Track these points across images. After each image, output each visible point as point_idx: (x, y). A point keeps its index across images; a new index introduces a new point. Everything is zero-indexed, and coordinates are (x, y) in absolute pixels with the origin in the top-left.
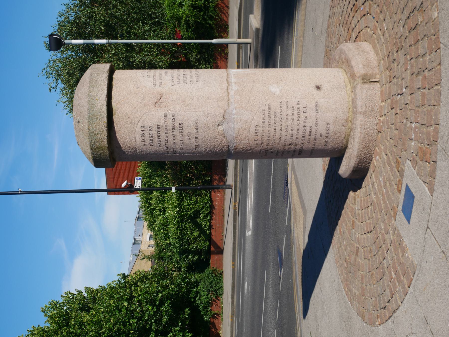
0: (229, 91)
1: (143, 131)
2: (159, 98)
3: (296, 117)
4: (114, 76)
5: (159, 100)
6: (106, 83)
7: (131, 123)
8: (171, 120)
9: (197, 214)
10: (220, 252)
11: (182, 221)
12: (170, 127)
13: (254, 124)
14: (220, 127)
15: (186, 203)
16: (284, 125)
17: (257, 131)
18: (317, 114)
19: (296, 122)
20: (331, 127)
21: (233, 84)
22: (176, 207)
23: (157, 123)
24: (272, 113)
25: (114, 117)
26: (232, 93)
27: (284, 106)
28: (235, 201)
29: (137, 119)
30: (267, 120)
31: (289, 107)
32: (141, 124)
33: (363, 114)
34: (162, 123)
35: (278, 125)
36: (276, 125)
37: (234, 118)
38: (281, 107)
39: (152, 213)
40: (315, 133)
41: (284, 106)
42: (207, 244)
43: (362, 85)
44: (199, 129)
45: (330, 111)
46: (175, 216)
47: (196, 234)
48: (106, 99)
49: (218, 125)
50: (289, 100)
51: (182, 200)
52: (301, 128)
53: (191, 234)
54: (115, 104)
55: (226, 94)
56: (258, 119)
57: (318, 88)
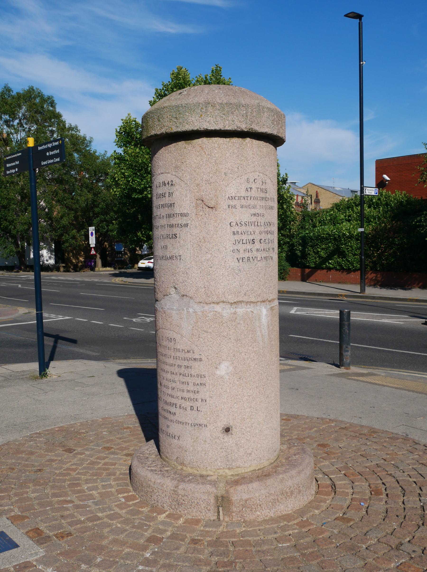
0: (221, 305)
1: (168, 184)
2: (209, 205)
3: (185, 395)
4: (248, 139)
5: (207, 206)
6: (228, 128)
7: (177, 167)
8: (180, 222)
9: (342, 254)
10: (304, 278)
11: (335, 239)
12: (173, 221)
13: (177, 337)
14: (174, 289)
15: (354, 244)
16: (177, 378)
17: (170, 340)
18: (190, 424)
19: (179, 394)
20: (176, 441)
21: (233, 311)
22: (350, 233)
23: (176, 203)
24: (191, 363)
25: (183, 142)
26: (218, 308)
27: (198, 381)
28: (346, 296)
29: (180, 174)
30: (181, 355)
31: (198, 387)
32: (176, 181)
33: (174, 491)
34: (177, 210)
35: (176, 370)
36: (176, 366)
37: (183, 310)
38: (198, 376)
39: (348, 208)
40: (170, 418)
41: (198, 381)
42: (313, 265)
43: (213, 495)
44: (170, 261)
45: (194, 442)
46: (340, 232)
47: (322, 254)
48: (202, 129)
49: (175, 288)
50: (207, 387)
51: (357, 240)
52: (173, 401)
53: (323, 249)
54: (200, 143)
55: (215, 299)
56: (183, 344)
57: (227, 430)
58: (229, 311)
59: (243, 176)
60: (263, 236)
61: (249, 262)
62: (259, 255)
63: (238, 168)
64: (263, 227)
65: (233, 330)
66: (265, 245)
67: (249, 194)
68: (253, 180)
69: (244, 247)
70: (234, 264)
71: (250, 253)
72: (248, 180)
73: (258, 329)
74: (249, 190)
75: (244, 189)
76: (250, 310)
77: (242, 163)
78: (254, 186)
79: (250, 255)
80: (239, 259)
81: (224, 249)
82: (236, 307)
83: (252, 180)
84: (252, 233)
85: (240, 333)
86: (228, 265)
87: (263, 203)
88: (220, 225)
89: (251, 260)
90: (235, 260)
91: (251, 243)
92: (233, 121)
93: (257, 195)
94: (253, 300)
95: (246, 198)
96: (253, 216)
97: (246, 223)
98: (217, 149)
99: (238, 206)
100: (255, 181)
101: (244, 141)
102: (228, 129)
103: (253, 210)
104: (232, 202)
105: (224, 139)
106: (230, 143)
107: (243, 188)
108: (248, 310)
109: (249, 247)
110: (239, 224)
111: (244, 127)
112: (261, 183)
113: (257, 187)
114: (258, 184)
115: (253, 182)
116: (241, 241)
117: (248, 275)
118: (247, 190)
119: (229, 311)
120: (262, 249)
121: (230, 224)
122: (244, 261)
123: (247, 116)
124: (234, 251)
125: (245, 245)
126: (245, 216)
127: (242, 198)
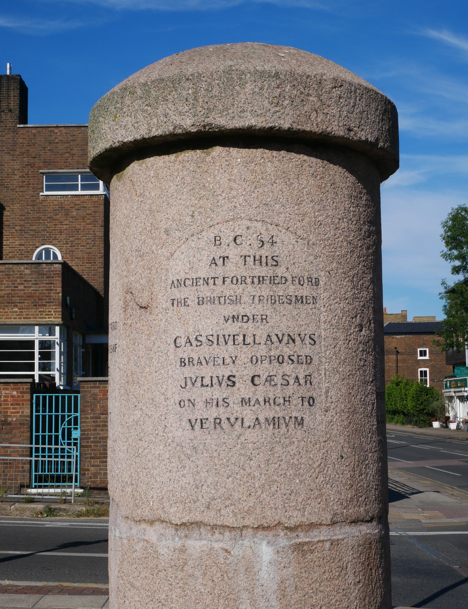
0: (157, 526)
4: (217, 150)
21: (178, 543)
26: (152, 533)
55: (147, 514)
58: (170, 544)
59: (204, 233)
60: (263, 370)
62: (248, 415)
63: (193, 216)
64: (263, 347)
65: (179, 590)
66: (272, 389)
67: (220, 271)
68: (232, 239)
69: (207, 393)
70: (181, 433)
71: (222, 409)
72: (217, 241)
73: (245, 595)
74: (220, 262)
75: (206, 260)
76: (221, 545)
77: (201, 202)
78: (233, 252)
79: (222, 412)
80: (193, 421)
81: (162, 398)
82: (186, 536)
83: (227, 238)
84: (228, 360)
85: (193, 598)
86: (170, 435)
87: (265, 290)
88: (156, 346)
89: (225, 425)
90: (183, 424)
91: (224, 384)
92: (166, 116)
93: (242, 272)
94: (230, 521)
96: (230, 321)
97: (211, 338)
98: (153, 180)
99: (192, 301)
100: (238, 241)
101: (208, 154)
102: (156, 134)
103: (230, 307)
104: (180, 291)
105: (166, 158)
106: (177, 163)
107: (205, 258)
108: (217, 546)
109: (217, 393)
110: (193, 341)
111: (188, 123)
112: (256, 244)
113: (244, 253)
114: (249, 246)
115: (232, 244)
116: (199, 380)
117: (216, 461)
119: (170, 544)
120: (261, 400)
122: (205, 426)
123: (196, 99)
124: (182, 404)
125: (209, 389)
126: (209, 322)
127: (201, 281)
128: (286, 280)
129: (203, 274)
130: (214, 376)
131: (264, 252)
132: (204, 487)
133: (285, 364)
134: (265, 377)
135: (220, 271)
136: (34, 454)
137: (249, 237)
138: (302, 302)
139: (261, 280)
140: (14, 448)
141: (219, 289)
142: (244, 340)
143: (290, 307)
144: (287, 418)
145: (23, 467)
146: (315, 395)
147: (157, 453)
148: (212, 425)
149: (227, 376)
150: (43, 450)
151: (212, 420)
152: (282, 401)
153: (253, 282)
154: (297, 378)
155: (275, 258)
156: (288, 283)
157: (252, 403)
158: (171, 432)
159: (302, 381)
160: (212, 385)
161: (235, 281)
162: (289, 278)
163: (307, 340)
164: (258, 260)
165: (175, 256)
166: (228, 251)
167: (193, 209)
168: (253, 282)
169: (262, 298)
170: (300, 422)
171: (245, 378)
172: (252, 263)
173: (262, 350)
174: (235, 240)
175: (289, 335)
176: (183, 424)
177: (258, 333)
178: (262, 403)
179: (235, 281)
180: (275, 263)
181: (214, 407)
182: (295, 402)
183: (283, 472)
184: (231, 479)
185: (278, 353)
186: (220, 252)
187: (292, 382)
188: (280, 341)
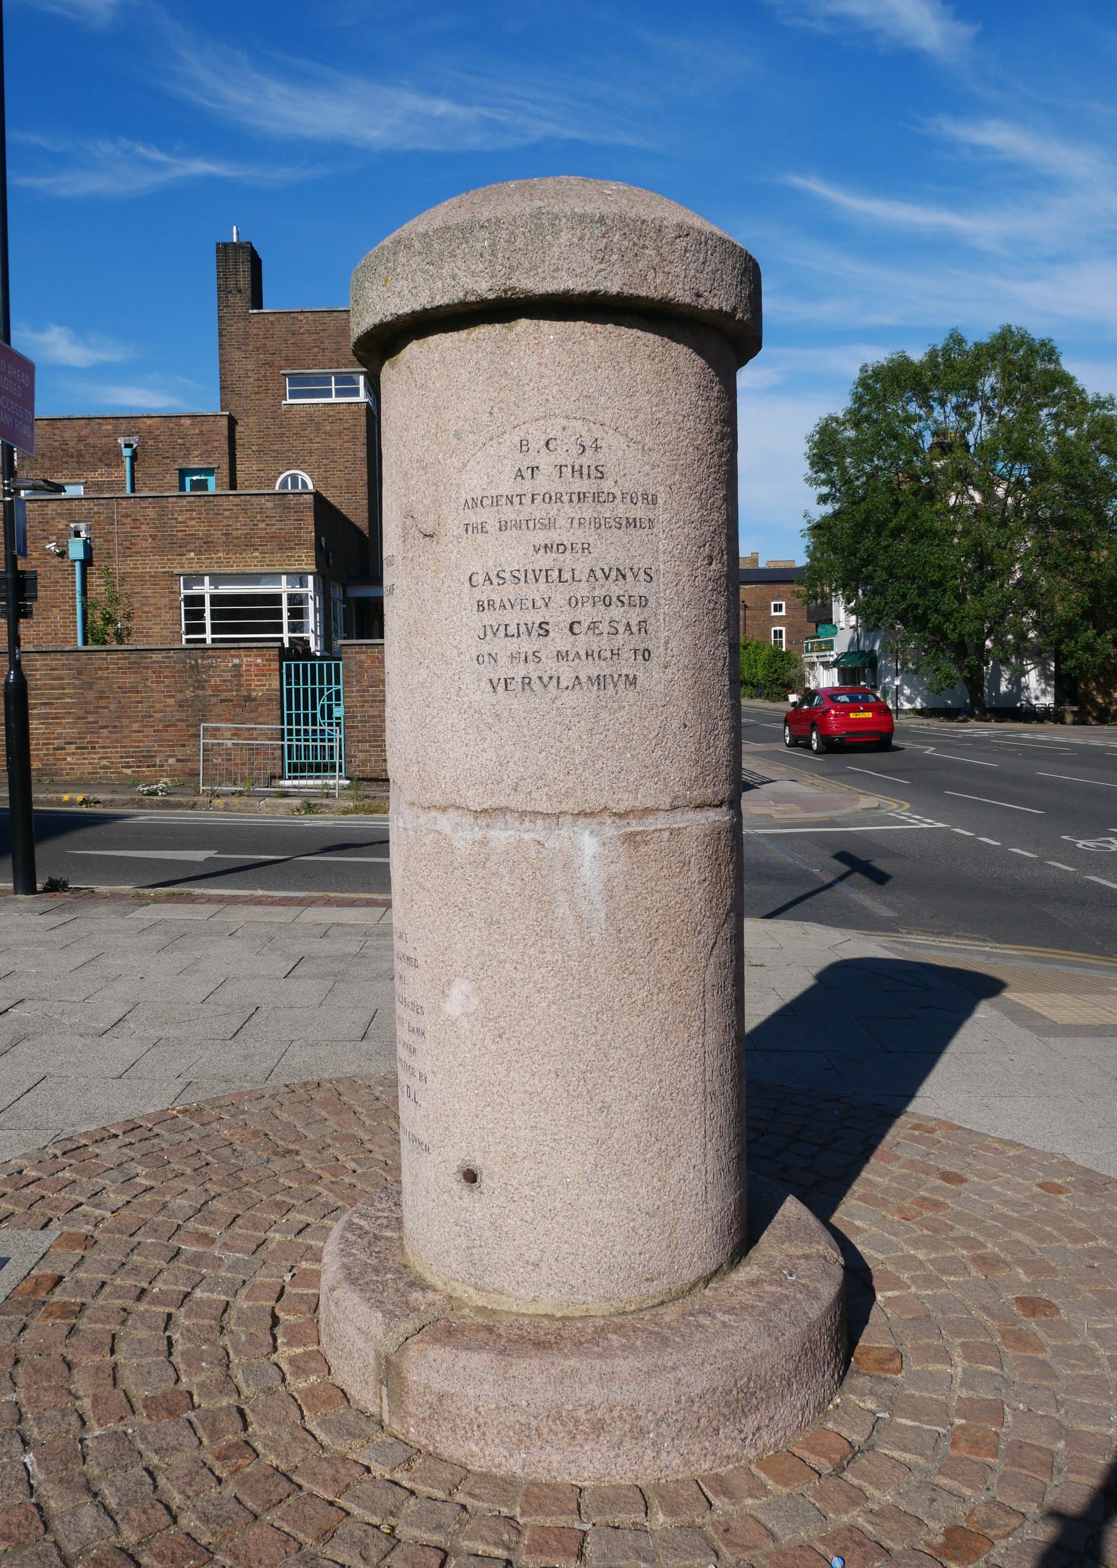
0: (452, 813)
4: (523, 324)
21: (478, 834)
26: (445, 823)
55: (438, 798)
59: (506, 436)
60: (585, 614)
61: (528, 692)
62: (566, 671)
63: (491, 413)
64: (584, 584)
66: (596, 639)
67: (527, 486)
68: (543, 443)
69: (513, 645)
70: (479, 696)
71: (531, 666)
72: (523, 446)
73: (562, 897)
75: (509, 471)
76: (532, 835)
77: (502, 394)
78: (545, 461)
80: (495, 682)
82: (488, 826)
86: (465, 699)
87: (587, 511)
88: (446, 585)
89: (536, 685)
90: (483, 684)
93: (556, 487)
94: (543, 806)
95: (516, 500)
96: (542, 551)
97: (516, 574)
100: (551, 446)
101: (510, 329)
102: (441, 302)
103: (542, 533)
105: (455, 334)
107: (508, 469)
108: (526, 837)
109: (526, 645)
112: (575, 450)
113: (559, 462)
115: (544, 450)
116: (502, 628)
117: (525, 731)
118: (520, 474)
119: (468, 834)
120: (582, 653)
121: (470, 579)
123: (493, 254)
124: (481, 659)
125: (515, 639)
126: (514, 552)
127: (504, 499)
128: (614, 497)
129: (505, 490)
130: (522, 623)
131: (587, 460)
132: (510, 764)
133: (613, 607)
134: (587, 624)
135: (527, 486)
136: (286, 737)
137: (566, 441)
138: (635, 526)
139: (582, 497)
140: (261, 729)
141: (528, 510)
142: (560, 577)
143: (620, 532)
144: (616, 676)
145: (273, 754)
146: (651, 647)
147: (450, 722)
148: (520, 686)
149: (538, 622)
150: (298, 732)
151: (520, 680)
152: (609, 654)
153: (571, 500)
154: (628, 625)
155: (600, 468)
156: (616, 501)
157: (571, 657)
158: (468, 695)
159: (635, 629)
160: (519, 635)
161: (547, 500)
162: (619, 495)
163: (642, 576)
164: (578, 471)
165: (469, 467)
166: (538, 459)
167: (491, 403)
168: (571, 500)
169: (582, 521)
170: (633, 682)
171: (561, 626)
172: (570, 475)
173: (583, 589)
174: (547, 444)
175: (618, 569)
176: (483, 684)
177: (578, 567)
178: (584, 657)
179: (547, 500)
180: (599, 475)
181: (522, 663)
182: (625, 656)
183: (611, 744)
184: (544, 754)
185: (603, 592)
186: (529, 461)
187: (621, 630)
188: (607, 578)
